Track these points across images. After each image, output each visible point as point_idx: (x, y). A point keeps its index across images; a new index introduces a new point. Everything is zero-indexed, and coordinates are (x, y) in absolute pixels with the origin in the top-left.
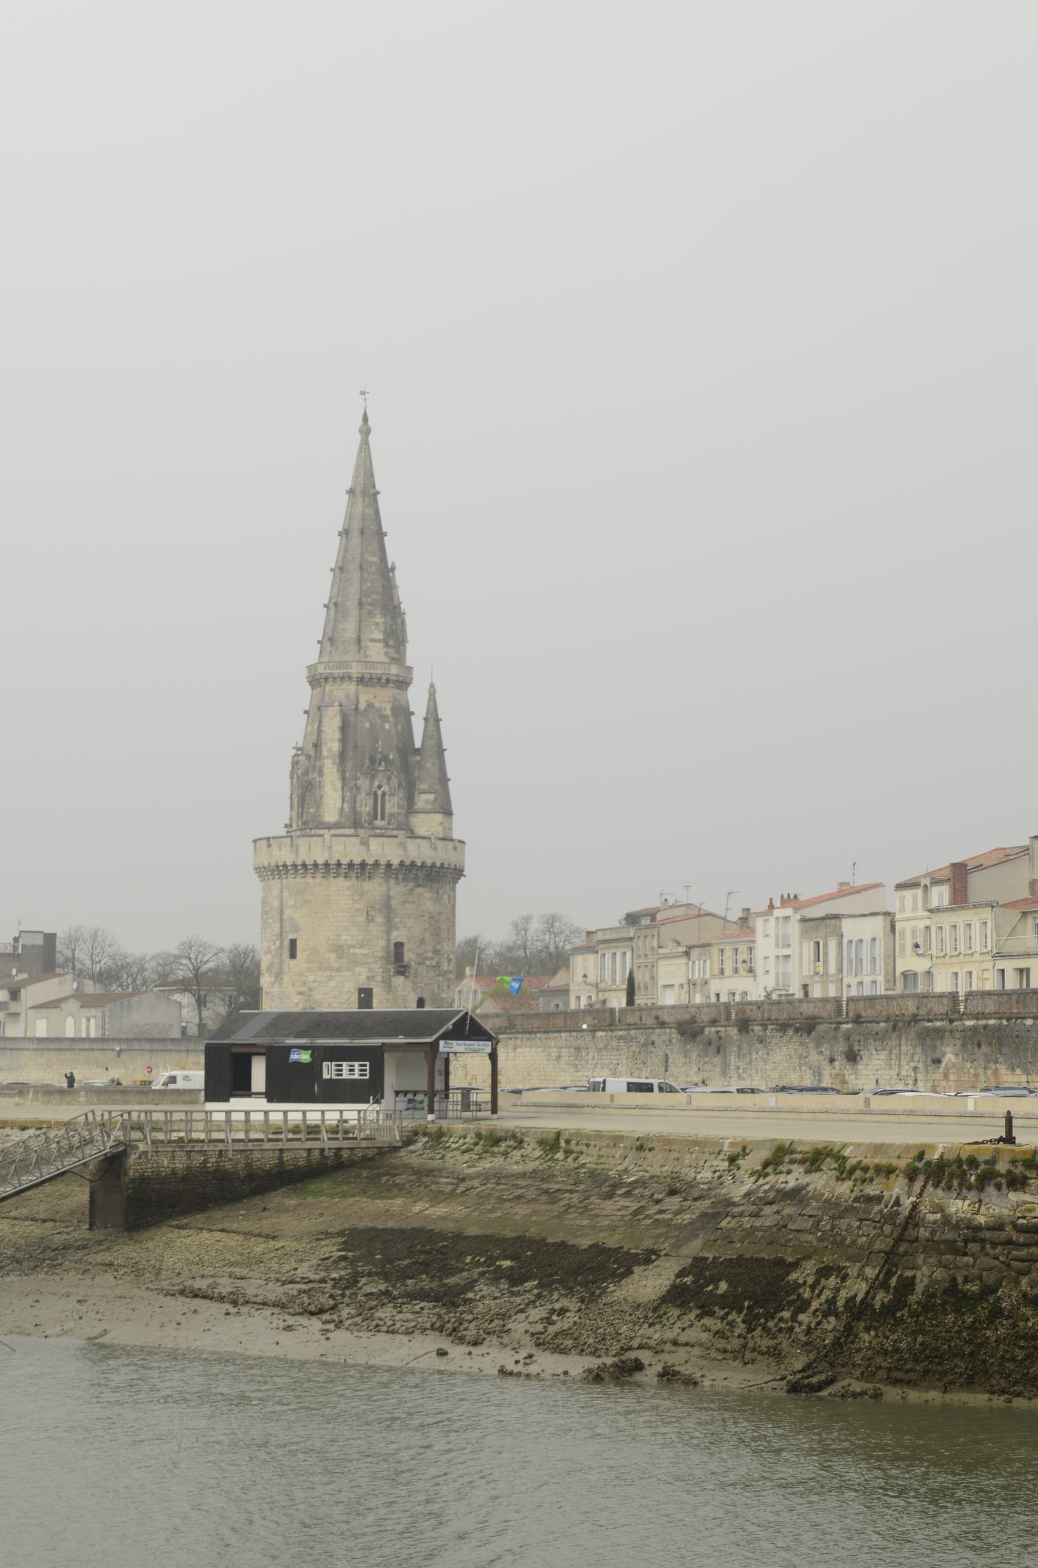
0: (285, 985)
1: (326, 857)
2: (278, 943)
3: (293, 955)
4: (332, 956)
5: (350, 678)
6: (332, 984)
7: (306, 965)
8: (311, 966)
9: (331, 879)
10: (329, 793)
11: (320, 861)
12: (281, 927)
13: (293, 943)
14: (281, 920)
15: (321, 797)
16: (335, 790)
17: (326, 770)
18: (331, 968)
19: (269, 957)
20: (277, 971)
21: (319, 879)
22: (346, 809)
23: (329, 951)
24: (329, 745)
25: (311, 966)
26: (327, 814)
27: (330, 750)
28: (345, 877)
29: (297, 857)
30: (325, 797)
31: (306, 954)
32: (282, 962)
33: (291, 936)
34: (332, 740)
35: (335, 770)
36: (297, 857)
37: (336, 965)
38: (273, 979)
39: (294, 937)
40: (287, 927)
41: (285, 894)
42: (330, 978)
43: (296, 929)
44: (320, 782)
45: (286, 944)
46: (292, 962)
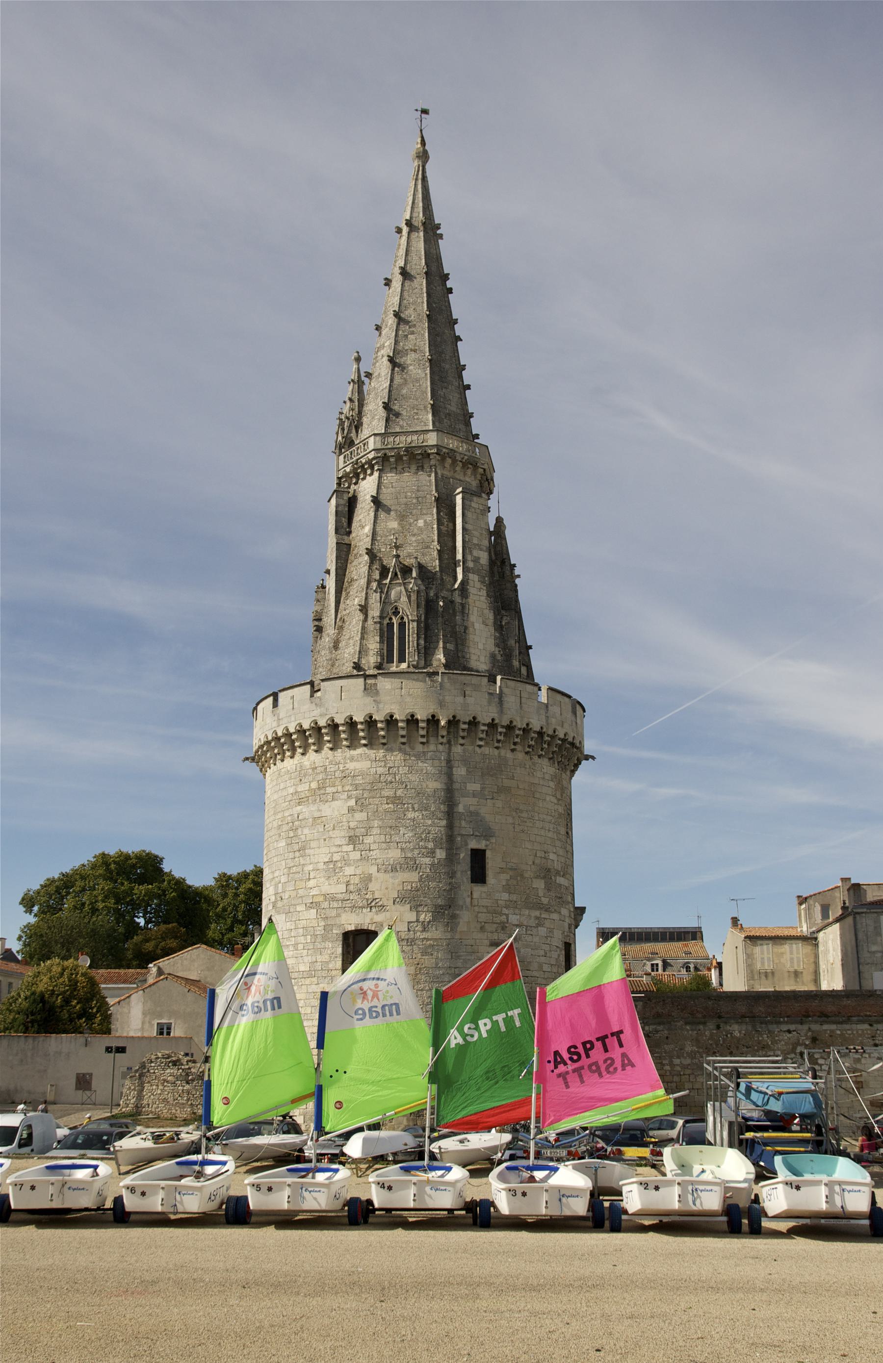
0: (462, 927)
1: (544, 723)
2: (441, 854)
3: (479, 875)
4: (540, 884)
5: (475, 466)
6: (542, 931)
7: (505, 896)
8: (514, 897)
9: (536, 758)
10: (477, 626)
11: (536, 725)
12: (450, 826)
13: (478, 858)
14: (450, 814)
15: (466, 628)
16: (484, 623)
17: (472, 590)
18: (540, 906)
19: (414, 876)
20: (440, 902)
21: (520, 756)
22: (499, 657)
23: (537, 877)
24: (476, 553)
25: (514, 897)
26: (474, 657)
27: (476, 560)
28: (550, 759)
29: (501, 711)
30: (471, 629)
31: (504, 877)
32: (453, 888)
33: (473, 844)
34: (479, 547)
35: (484, 593)
36: (501, 711)
37: (545, 901)
38: (425, 917)
39: (482, 845)
40: (464, 826)
41: (460, 772)
42: (540, 922)
43: (487, 833)
44: (463, 606)
45: (464, 856)
46: (478, 889)
